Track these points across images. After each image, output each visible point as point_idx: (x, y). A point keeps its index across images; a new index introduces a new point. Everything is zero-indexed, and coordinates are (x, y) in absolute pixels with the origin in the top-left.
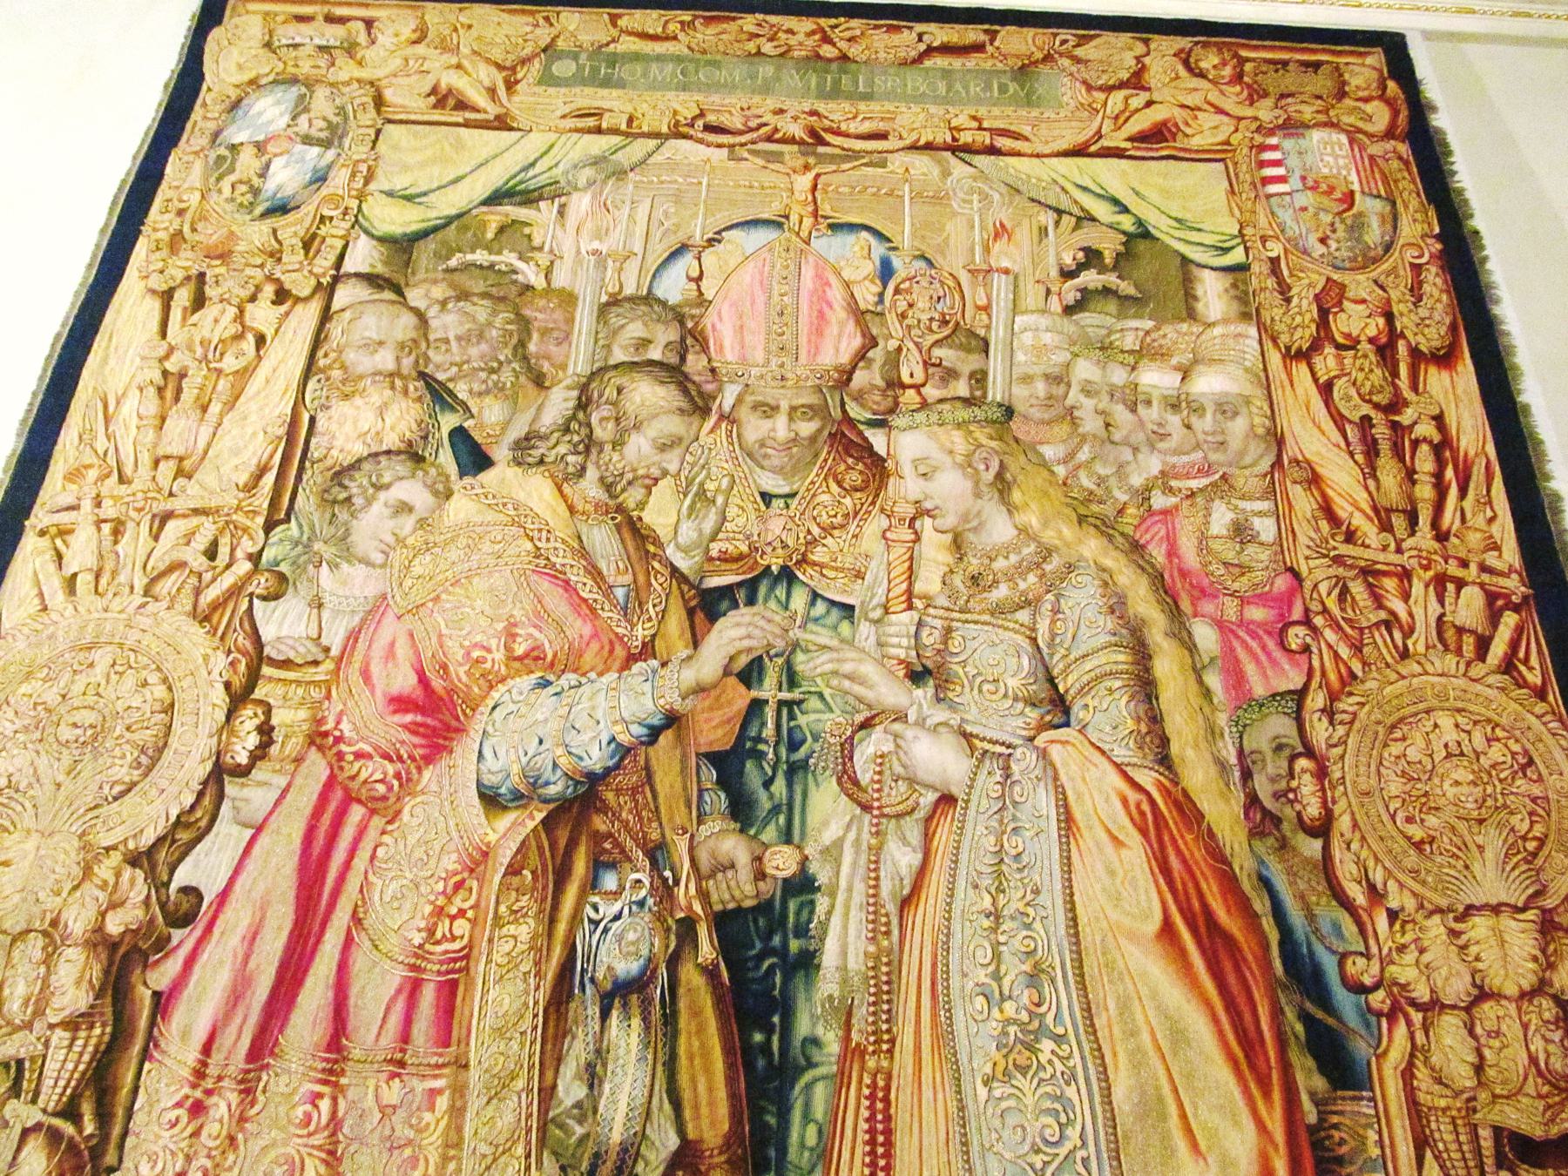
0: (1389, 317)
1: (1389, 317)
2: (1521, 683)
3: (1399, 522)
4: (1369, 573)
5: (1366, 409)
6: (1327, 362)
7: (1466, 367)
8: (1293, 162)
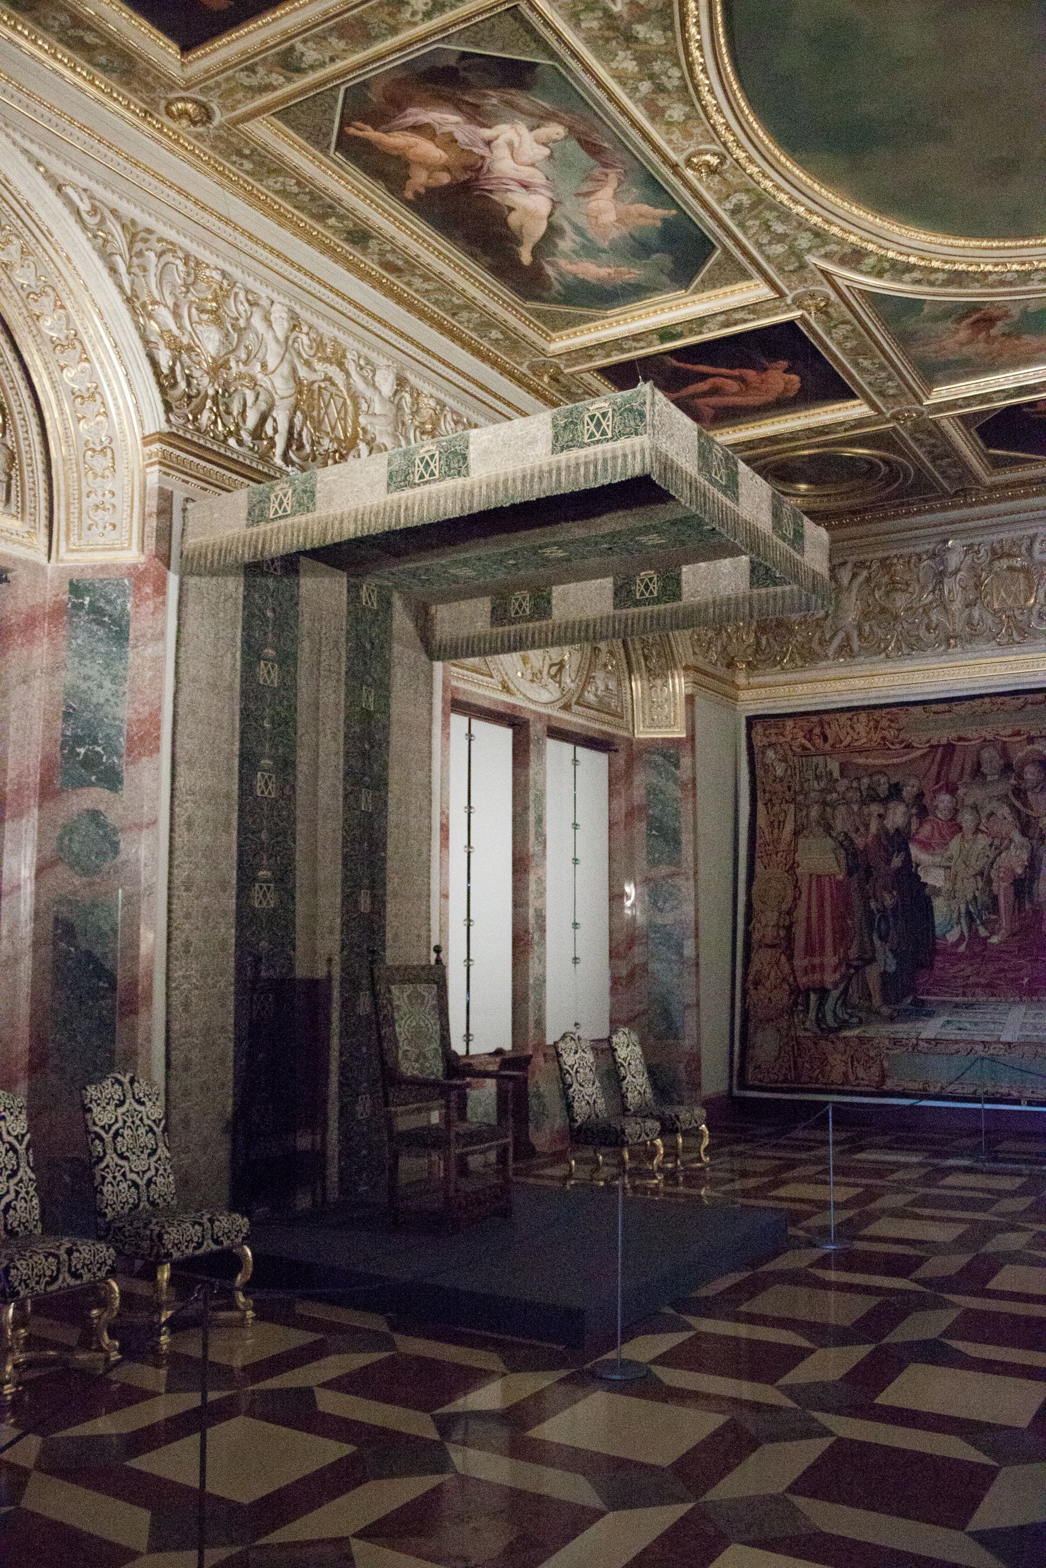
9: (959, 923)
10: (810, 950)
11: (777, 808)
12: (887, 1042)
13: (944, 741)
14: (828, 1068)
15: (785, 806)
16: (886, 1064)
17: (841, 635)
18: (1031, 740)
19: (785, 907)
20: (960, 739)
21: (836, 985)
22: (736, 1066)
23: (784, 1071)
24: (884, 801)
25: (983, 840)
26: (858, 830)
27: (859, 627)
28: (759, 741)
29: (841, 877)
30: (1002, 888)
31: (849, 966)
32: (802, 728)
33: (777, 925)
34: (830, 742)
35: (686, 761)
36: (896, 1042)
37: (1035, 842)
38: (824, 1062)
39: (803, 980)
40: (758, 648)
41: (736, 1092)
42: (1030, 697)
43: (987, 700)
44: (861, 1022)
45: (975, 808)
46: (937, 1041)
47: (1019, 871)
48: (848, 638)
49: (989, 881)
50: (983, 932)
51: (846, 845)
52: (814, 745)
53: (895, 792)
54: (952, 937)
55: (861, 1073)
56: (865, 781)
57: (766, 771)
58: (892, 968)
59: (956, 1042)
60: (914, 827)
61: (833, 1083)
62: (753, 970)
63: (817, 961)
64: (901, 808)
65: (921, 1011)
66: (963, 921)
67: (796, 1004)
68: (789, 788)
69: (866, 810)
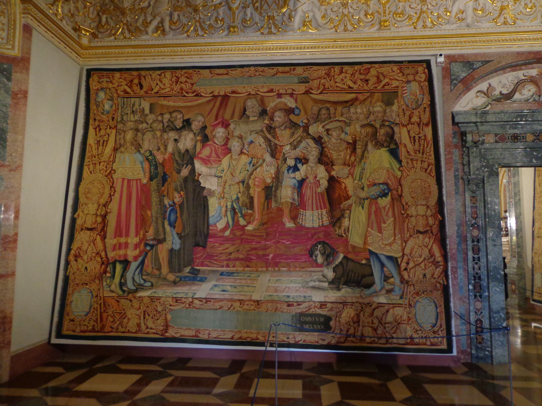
0: (420, 118)
1: (420, 118)
2: (431, 175)
3: (418, 152)
4: (412, 160)
5: (414, 135)
6: (410, 127)
7: (430, 128)
8: (408, 89)
9: (226, 215)
10: (118, 233)
11: (103, 132)
12: (170, 300)
13: (222, 93)
14: (126, 321)
15: (108, 131)
16: (169, 317)
17: (158, 19)
18: (280, 95)
19: (102, 201)
20: (233, 92)
21: (136, 258)
22: (56, 319)
23: (92, 323)
24: (179, 130)
25: (244, 159)
26: (159, 149)
27: (171, 15)
28: (94, 85)
29: (145, 181)
30: (256, 192)
31: (146, 245)
32: (125, 79)
33: (97, 215)
34: (145, 89)
35: (16, 76)
36: (177, 300)
37: (280, 162)
38: (123, 315)
39: (111, 255)
40: (99, 25)
41: (54, 341)
42: (281, 69)
43: (252, 68)
44: (152, 285)
45: (241, 137)
46: (207, 300)
47: (269, 181)
48: (162, 22)
49: (248, 187)
50: (242, 222)
51: (150, 159)
52: (133, 91)
53: (187, 123)
54: (221, 225)
55: (150, 324)
56: (167, 116)
57: (98, 106)
58: (177, 247)
59: (221, 300)
60: (198, 150)
61: (129, 331)
62: (75, 246)
63: (123, 240)
64: (191, 135)
65: (196, 277)
66: (229, 213)
67: (105, 272)
68: (113, 119)
69: (165, 136)
